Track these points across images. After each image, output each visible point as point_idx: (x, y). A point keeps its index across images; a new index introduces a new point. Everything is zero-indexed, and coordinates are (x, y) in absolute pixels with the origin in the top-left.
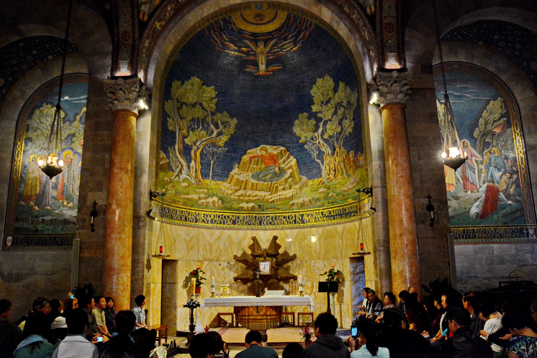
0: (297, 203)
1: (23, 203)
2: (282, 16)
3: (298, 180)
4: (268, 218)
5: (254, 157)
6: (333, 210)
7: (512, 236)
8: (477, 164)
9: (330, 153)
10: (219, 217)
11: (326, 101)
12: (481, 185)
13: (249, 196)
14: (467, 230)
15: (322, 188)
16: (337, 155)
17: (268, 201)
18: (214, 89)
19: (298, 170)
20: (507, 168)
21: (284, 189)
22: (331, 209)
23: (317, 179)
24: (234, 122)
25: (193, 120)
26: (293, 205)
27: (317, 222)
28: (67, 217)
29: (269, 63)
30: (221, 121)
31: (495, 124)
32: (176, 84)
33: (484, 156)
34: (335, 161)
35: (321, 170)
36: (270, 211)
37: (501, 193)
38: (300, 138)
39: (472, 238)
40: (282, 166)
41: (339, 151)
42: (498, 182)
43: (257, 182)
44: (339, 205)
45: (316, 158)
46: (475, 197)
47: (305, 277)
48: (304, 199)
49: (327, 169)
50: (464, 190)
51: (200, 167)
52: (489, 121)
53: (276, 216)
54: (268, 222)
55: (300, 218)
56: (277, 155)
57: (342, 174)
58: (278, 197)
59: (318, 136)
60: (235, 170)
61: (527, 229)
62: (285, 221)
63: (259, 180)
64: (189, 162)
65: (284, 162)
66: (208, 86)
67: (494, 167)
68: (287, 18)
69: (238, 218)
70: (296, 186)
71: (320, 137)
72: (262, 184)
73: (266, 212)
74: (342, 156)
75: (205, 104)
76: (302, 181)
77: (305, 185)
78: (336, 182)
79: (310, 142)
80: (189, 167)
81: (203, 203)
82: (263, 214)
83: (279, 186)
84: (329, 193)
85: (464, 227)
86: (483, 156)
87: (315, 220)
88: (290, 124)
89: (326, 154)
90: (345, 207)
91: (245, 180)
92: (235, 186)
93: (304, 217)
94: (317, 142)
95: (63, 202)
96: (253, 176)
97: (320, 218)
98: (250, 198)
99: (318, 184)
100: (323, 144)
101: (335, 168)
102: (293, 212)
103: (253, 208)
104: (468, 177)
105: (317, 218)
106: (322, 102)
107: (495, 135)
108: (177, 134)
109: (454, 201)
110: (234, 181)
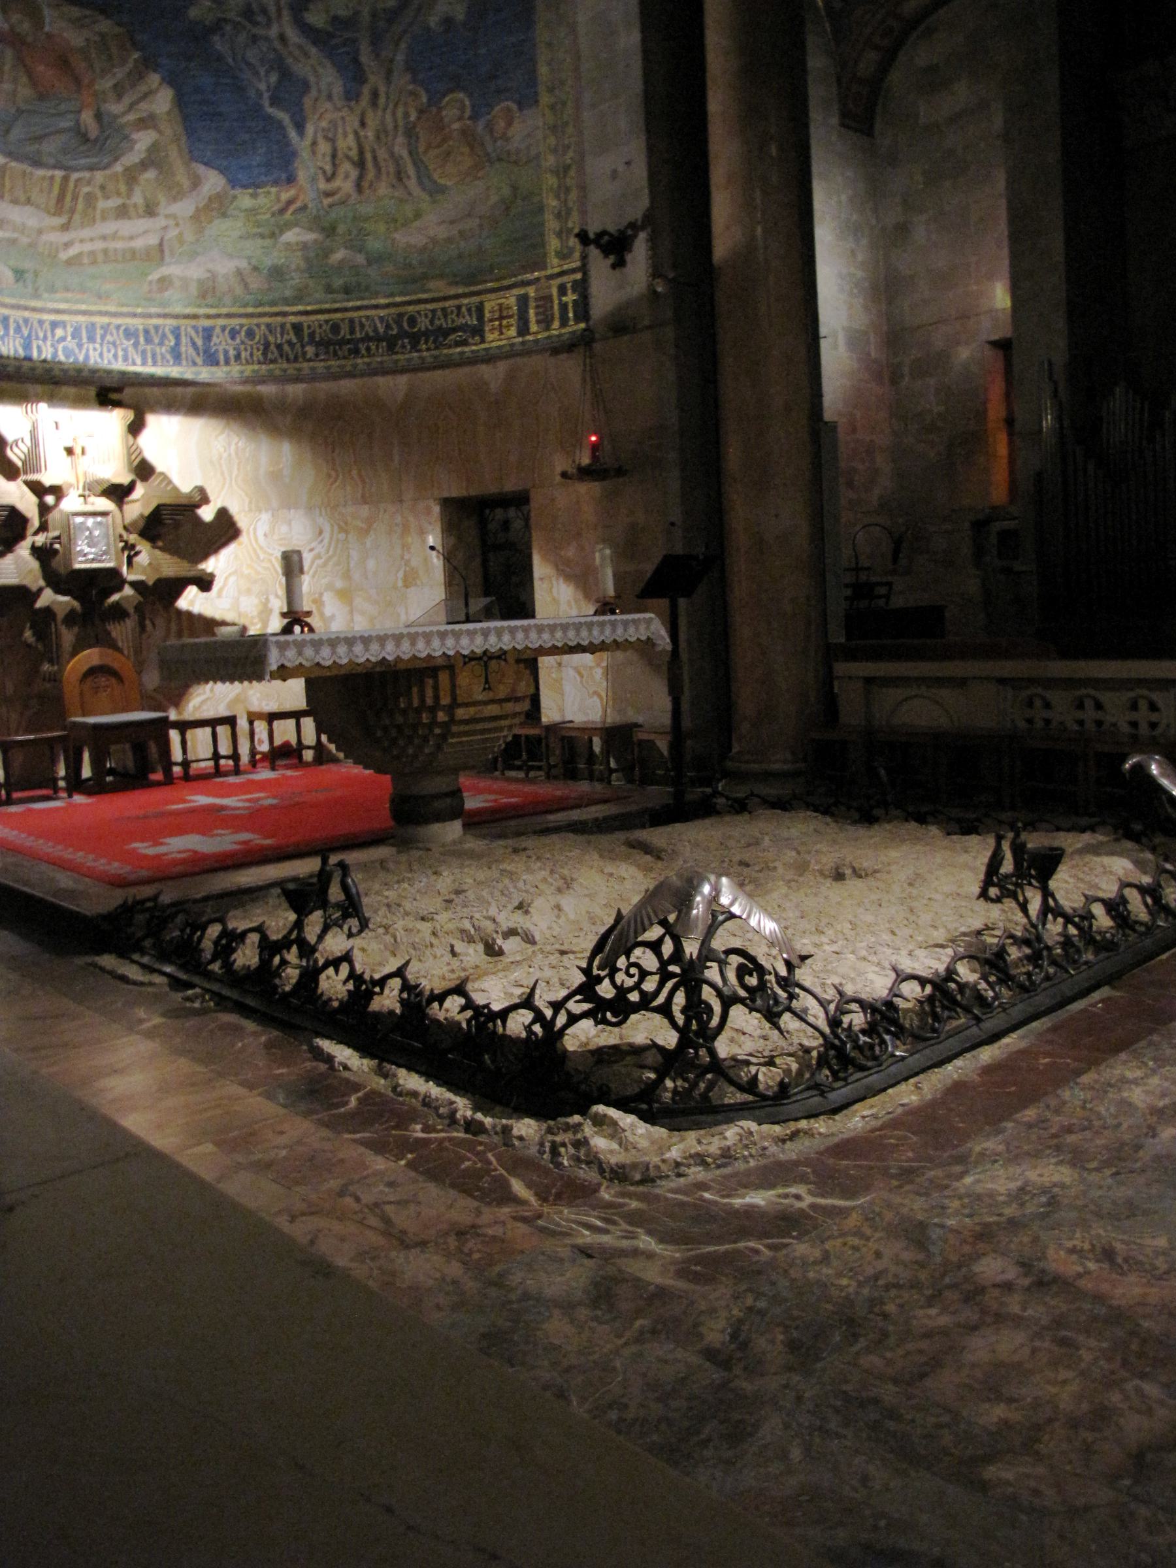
0: (185, 282)
3: (186, 183)
4: (59, 332)
6: (352, 321)
9: (338, 89)
15: (296, 230)
16: (374, 103)
17: (53, 256)
19: (184, 139)
21: (122, 212)
22: (338, 315)
23: (274, 190)
26: (164, 283)
27: (273, 361)
34: (363, 124)
35: (294, 154)
36: (67, 301)
40: (115, 108)
41: (382, 90)
44: (382, 301)
45: (266, 102)
47: (232, 579)
48: (210, 266)
49: (319, 156)
53: (93, 325)
54: (60, 347)
55: (199, 342)
57: (400, 179)
58: (99, 245)
59: (279, 10)
62: (131, 349)
65: (119, 91)
71: (286, 16)
72: (24, 173)
73: (50, 305)
74: (400, 112)
77: (217, 207)
78: (367, 209)
79: (237, 26)
82: (34, 310)
83: (99, 194)
84: (327, 253)
87: (265, 354)
89: (314, 93)
90: (411, 308)
93: (215, 340)
94: (274, 32)
97: (286, 348)
99: (276, 208)
100: (300, 47)
101: (361, 152)
102: (165, 316)
105: (272, 347)
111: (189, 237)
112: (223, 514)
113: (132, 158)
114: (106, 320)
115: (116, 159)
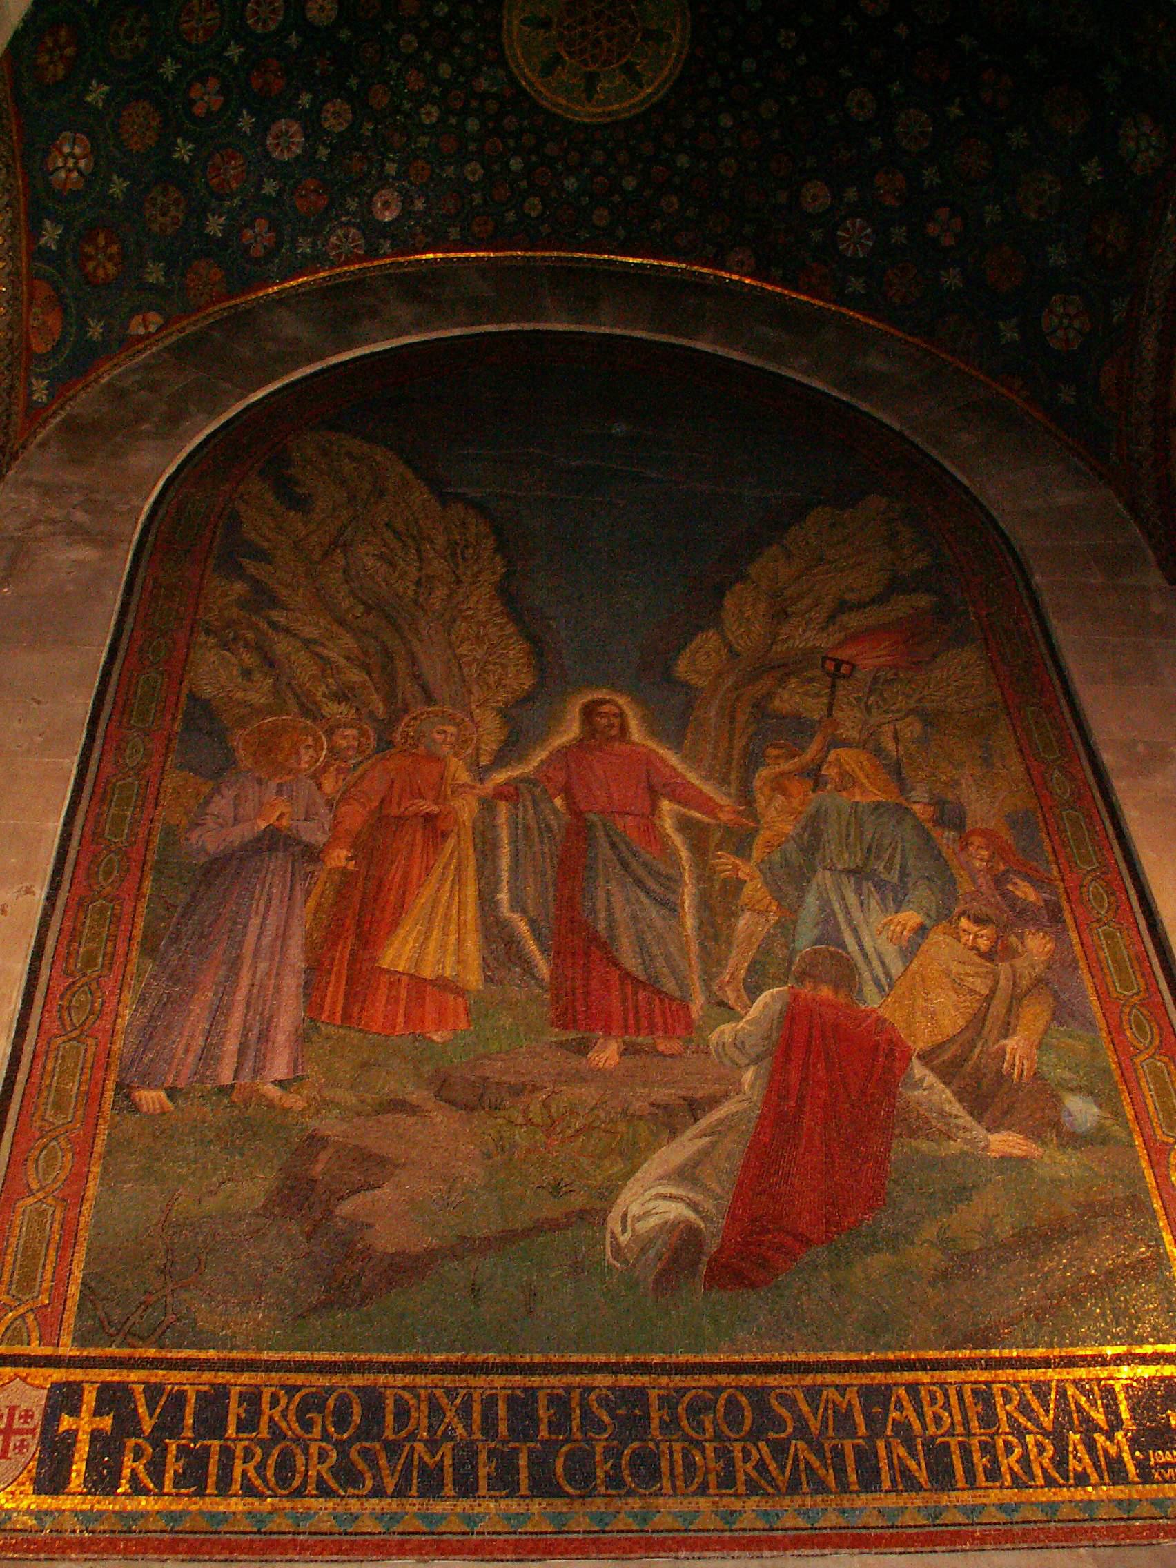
7: (1061, 1461)
8: (699, 847)
12: (731, 996)
14: (559, 1402)
20: (964, 886)
31: (853, 621)
33: (762, 801)
37: (918, 1070)
39: (615, 1481)
42: (886, 987)
46: (661, 1094)
50: (555, 1035)
52: (808, 601)
67: (849, 872)
85: (529, 1369)
86: (746, 797)
104: (601, 927)
107: (844, 676)
109: (442, 1119)
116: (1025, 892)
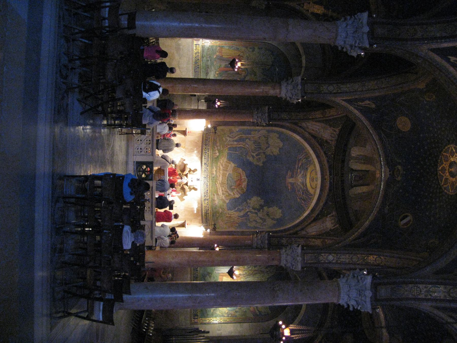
1: (218, 48)
2: (311, 191)
3: (227, 198)
4: (207, 182)
5: (240, 174)
9: (240, 215)
10: (208, 156)
11: (268, 214)
13: (219, 172)
16: (238, 218)
18: (278, 154)
21: (222, 190)
22: (210, 214)
24: (261, 164)
25: (259, 143)
26: (214, 195)
28: (210, 73)
29: (292, 184)
30: (260, 157)
32: (278, 136)
35: (231, 210)
38: (250, 200)
40: (235, 190)
43: (227, 176)
51: (234, 147)
56: (241, 187)
58: (218, 188)
60: (233, 165)
61: (197, 318)
63: (228, 177)
64: (236, 141)
65: (237, 191)
66: (279, 151)
68: (311, 194)
69: (208, 166)
70: (224, 197)
71: (249, 210)
75: (269, 149)
76: (226, 200)
77: (224, 202)
80: (234, 141)
81: (215, 148)
88: (258, 195)
91: (228, 170)
92: (225, 164)
95: (218, 71)
96: (229, 174)
98: (218, 173)
103: (213, 174)
106: (268, 212)
108: (250, 136)
110: (228, 164)
111: (220, 198)
112: (184, 200)
113: (229, 192)
114: (209, 188)
115: (229, 190)
116: (230, 315)
